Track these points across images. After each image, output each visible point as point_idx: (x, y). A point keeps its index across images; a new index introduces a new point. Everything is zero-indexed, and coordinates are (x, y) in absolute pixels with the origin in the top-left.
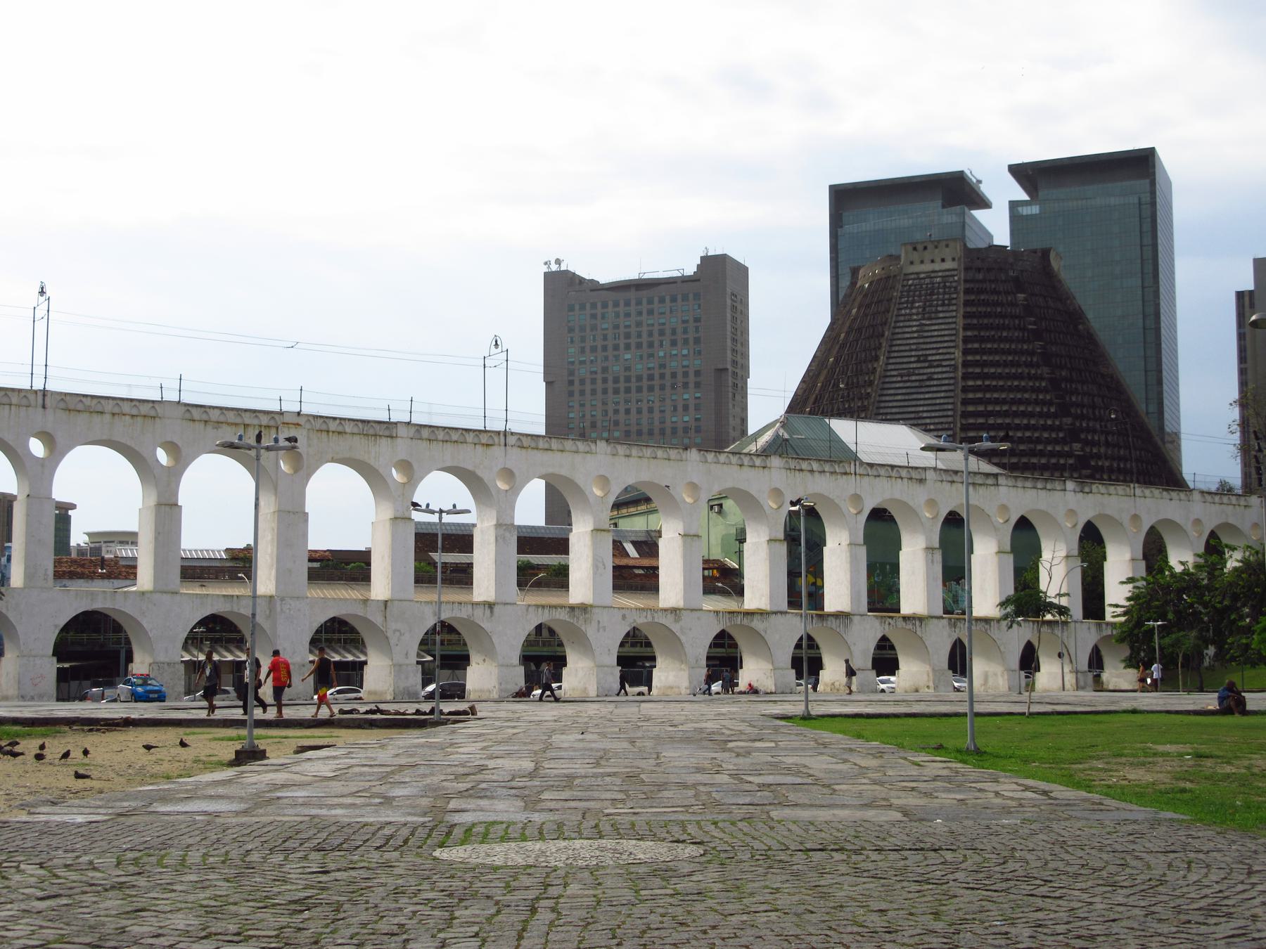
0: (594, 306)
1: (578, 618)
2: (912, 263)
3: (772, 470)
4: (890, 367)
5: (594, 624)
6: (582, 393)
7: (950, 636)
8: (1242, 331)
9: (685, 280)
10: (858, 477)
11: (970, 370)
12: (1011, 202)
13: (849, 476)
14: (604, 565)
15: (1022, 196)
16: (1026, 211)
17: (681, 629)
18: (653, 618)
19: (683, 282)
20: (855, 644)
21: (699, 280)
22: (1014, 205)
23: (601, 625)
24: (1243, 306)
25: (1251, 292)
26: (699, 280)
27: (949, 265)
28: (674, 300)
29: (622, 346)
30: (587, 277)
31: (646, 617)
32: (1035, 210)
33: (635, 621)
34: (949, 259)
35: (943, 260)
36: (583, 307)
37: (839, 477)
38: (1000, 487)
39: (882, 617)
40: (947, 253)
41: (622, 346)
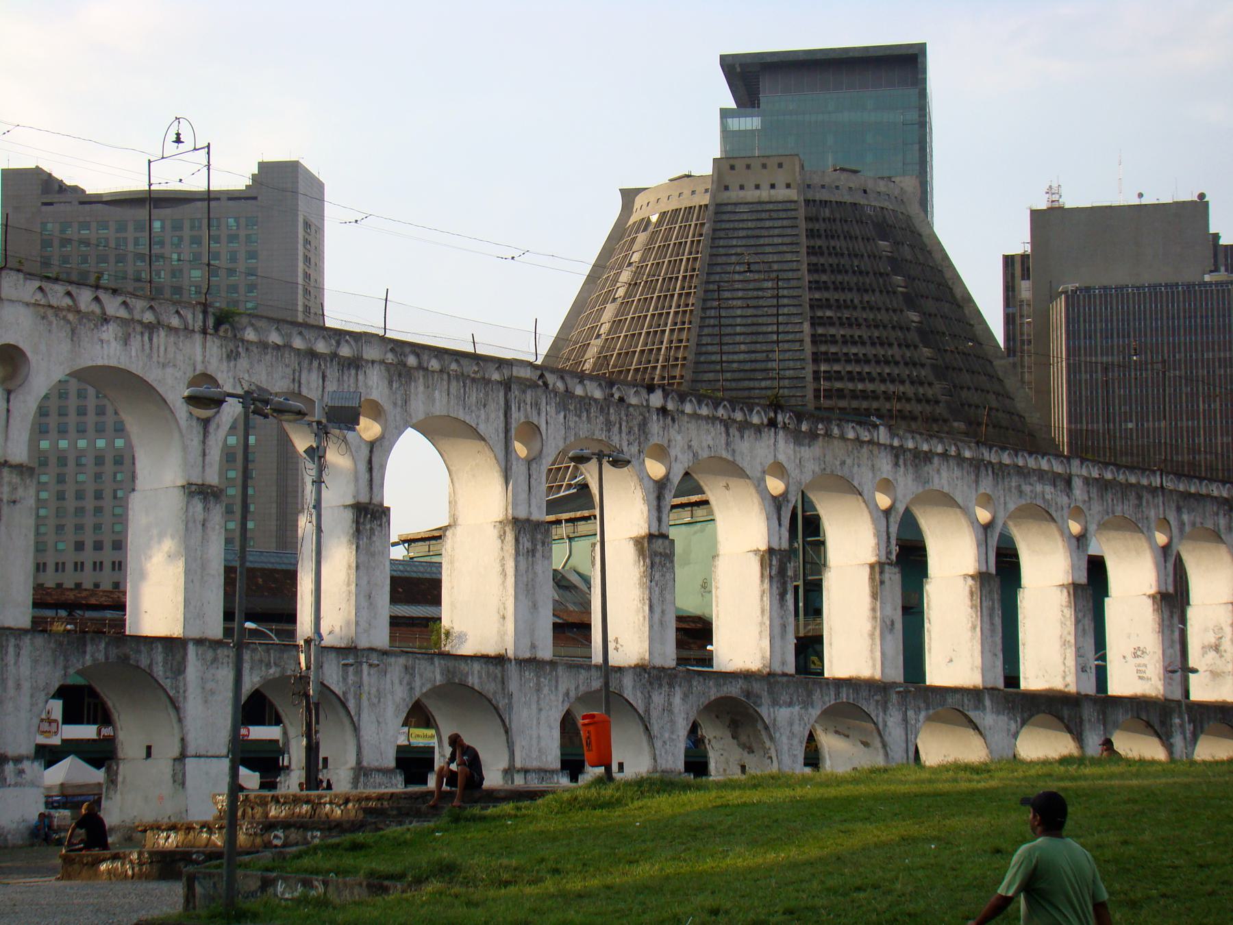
2: (726, 188)
4: (705, 340)
8: (1011, 310)
9: (233, 197)
11: (823, 348)
12: (722, 110)
15: (731, 104)
16: (735, 124)
19: (230, 199)
21: (255, 198)
22: (725, 114)
24: (1013, 276)
25: (1024, 257)
26: (255, 198)
27: (781, 193)
30: (68, 182)
32: (751, 123)
34: (781, 184)
35: (773, 186)
40: (781, 177)
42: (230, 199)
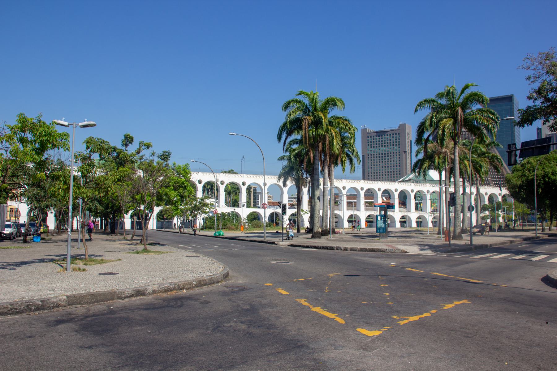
0: (374, 137)
6: (371, 157)
28: (393, 134)
29: (381, 146)
36: (371, 137)
41: (381, 146)
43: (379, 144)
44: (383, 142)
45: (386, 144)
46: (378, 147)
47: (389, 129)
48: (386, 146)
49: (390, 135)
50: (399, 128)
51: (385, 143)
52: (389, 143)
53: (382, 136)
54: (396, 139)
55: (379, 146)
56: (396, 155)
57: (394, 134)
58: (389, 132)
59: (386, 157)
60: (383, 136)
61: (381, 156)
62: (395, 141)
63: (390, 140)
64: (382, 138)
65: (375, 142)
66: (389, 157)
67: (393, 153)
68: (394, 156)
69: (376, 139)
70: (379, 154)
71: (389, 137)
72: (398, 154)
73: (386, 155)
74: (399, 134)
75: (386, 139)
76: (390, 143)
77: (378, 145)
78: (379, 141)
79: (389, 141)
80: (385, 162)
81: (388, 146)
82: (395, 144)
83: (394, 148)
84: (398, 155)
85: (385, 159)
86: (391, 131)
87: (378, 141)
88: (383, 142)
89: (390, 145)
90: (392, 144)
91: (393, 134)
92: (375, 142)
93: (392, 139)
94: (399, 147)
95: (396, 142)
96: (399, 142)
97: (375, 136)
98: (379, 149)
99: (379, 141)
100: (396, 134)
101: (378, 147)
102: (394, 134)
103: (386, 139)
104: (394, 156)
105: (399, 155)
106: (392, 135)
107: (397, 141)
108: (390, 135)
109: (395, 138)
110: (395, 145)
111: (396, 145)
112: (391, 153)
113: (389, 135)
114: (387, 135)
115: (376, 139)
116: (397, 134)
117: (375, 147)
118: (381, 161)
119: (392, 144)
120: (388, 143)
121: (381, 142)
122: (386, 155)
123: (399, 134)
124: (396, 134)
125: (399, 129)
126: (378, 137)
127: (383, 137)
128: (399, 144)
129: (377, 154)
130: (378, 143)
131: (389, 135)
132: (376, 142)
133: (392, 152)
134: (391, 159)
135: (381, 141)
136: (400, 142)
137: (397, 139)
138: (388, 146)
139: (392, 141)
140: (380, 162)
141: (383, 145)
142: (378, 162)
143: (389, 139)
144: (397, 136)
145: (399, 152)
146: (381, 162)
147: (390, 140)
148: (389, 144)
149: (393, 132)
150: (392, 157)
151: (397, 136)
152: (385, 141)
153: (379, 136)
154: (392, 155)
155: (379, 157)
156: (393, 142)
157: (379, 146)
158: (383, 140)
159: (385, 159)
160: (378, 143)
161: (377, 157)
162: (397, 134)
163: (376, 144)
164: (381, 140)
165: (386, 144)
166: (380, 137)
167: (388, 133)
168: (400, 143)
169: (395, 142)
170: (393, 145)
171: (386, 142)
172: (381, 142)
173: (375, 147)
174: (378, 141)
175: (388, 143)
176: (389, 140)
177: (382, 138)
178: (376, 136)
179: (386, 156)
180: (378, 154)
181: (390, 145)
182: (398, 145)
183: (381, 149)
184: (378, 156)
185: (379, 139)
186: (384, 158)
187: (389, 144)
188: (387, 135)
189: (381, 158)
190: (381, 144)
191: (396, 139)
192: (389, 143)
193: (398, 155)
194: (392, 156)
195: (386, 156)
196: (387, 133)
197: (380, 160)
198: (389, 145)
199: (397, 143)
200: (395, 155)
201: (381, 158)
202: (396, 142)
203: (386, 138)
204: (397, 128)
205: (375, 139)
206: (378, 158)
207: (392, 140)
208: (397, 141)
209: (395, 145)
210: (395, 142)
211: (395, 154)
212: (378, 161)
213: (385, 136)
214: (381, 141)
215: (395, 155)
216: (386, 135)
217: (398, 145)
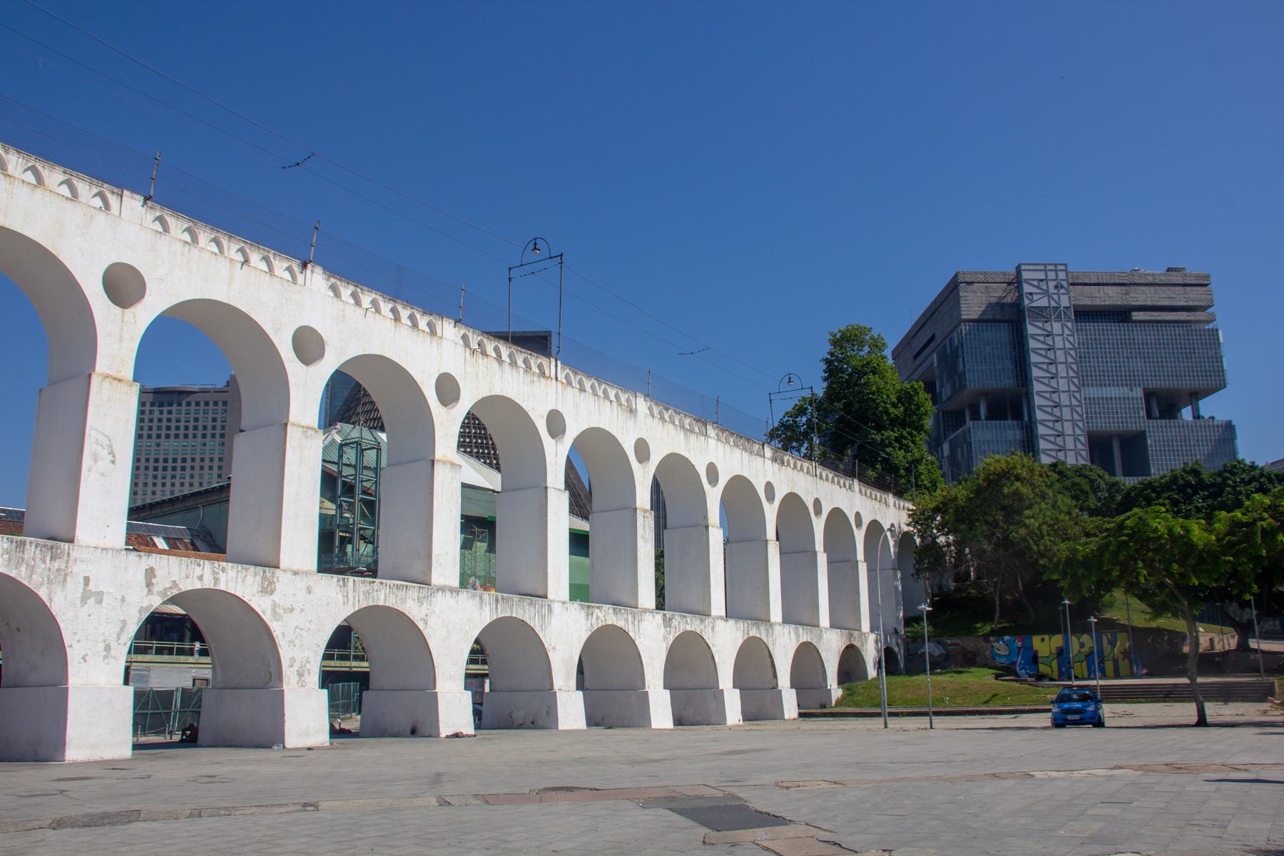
1: (32, 570)
3: (444, 340)
5: (74, 588)
7: (665, 639)
10: (559, 384)
13: (549, 381)
14: (112, 453)
17: (275, 605)
18: (216, 580)
19: (215, 392)
20: (554, 648)
23: (92, 587)
28: (207, 404)
29: (163, 436)
31: (201, 578)
33: (175, 584)
37: (536, 379)
38: (709, 439)
39: (589, 607)
42: (215, 392)
43: (159, 428)
44: (173, 424)
45: (182, 431)
46: (154, 436)
47: (196, 388)
48: (181, 436)
49: (198, 404)
50: (228, 386)
51: (178, 428)
52: (191, 428)
53: (171, 405)
54: (214, 420)
55: (159, 436)
56: (211, 468)
57: (211, 403)
58: (194, 395)
59: (178, 472)
60: (175, 405)
61: (161, 464)
62: (210, 424)
63: (196, 420)
64: (170, 412)
65: (147, 420)
66: (188, 471)
67: (202, 460)
68: (202, 468)
69: (151, 412)
70: (157, 460)
71: (192, 412)
72: (216, 463)
73: (179, 464)
74: (225, 403)
75: (183, 416)
76: (196, 428)
77: (154, 433)
78: (160, 420)
79: (192, 424)
80: (173, 485)
81: (186, 436)
82: (209, 432)
83: (204, 445)
84: (216, 468)
85: (174, 477)
86: (203, 391)
87: (156, 420)
88: (173, 424)
89: (195, 436)
90: (200, 432)
91: (207, 404)
92: (147, 420)
93: (201, 416)
94: (223, 444)
95: (214, 428)
96: (223, 427)
97: (148, 404)
98: (158, 445)
99: (160, 420)
100: (216, 404)
101: (154, 436)
102: (211, 403)
103: (183, 416)
104: (202, 468)
105: (220, 468)
106: (202, 404)
107: (219, 424)
108: (198, 404)
109: (210, 416)
110: (209, 436)
111: (214, 436)
112: (193, 460)
113: (193, 404)
114: (189, 404)
115: (151, 412)
116: (220, 403)
117: (145, 436)
118: (159, 482)
119: (200, 432)
120: (187, 428)
121: (164, 424)
122: (179, 464)
123: (225, 403)
124: (216, 404)
125: (226, 389)
126: (156, 409)
127: (174, 408)
128: (222, 436)
129: (148, 460)
130: (155, 424)
131: (193, 404)
132: (151, 420)
133: (198, 457)
134: (192, 477)
135: (165, 420)
136: (226, 428)
137: (219, 419)
138: (186, 436)
139: (200, 424)
140: (155, 484)
141: (173, 432)
142: (150, 485)
143: (192, 417)
144: (220, 411)
145: (221, 459)
146: (159, 484)
147: (196, 420)
148: (191, 431)
149: (207, 397)
150: (197, 472)
151: (220, 411)
152: (178, 421)
153: (161, 405)
154: (197, 464)
155: (156, 469)
156: (205, 428)
157: (159, 436)
158: (173, 416)
159: (174, 477)
160: (155, 424)
161: (147, 468)
162: (220, 403)
163: (150, 428)
164: (165, 416)
165: (182, 431)
166: (165, 409)
167: (192, 398)
168: (226, 432)
169: (209, 427)
170: (204, 436)
171: (182, 424)
172: (164, 424)
173: (145, 436)
174: (156, 420)
175: (187, 428)
176: (192, 420)
177: (170, 412)
178: (152, 404)
179: (179, 469)
180: (152, 460)
181: (195, 436)
182: (218, 436)
183: (165, 443)
184: (151, 464)
185: (161, 413)
186: (169, 473)
187: (191, 431)
188: (189, 404)
189: (160, 473)
190: (164, 428)
191: (214, 420)
192: (191, 428)
193: (216, 468)
194: (197, 468)
195: (179, 469)
196: (188, 399)
197: (155, 477)
198: (191, 436)
199: (218, 432)
200: (206, 468)
201: (160, 473)
202: (214, 428)
203: (183, 412)
204: (221, 384)
205: (147, 412)
206: (151, 472)
207: (201, 420)
208: (219, 424)
209: (209, 436)
210: (209, 427)
211: (207, 463)
212: (150, 481)
213: (180, 405)
214: (165, 420)
215: (206, 468)
216: (184, 403)
217: (218, 436)
